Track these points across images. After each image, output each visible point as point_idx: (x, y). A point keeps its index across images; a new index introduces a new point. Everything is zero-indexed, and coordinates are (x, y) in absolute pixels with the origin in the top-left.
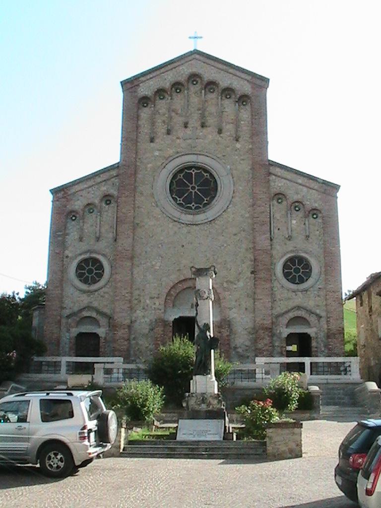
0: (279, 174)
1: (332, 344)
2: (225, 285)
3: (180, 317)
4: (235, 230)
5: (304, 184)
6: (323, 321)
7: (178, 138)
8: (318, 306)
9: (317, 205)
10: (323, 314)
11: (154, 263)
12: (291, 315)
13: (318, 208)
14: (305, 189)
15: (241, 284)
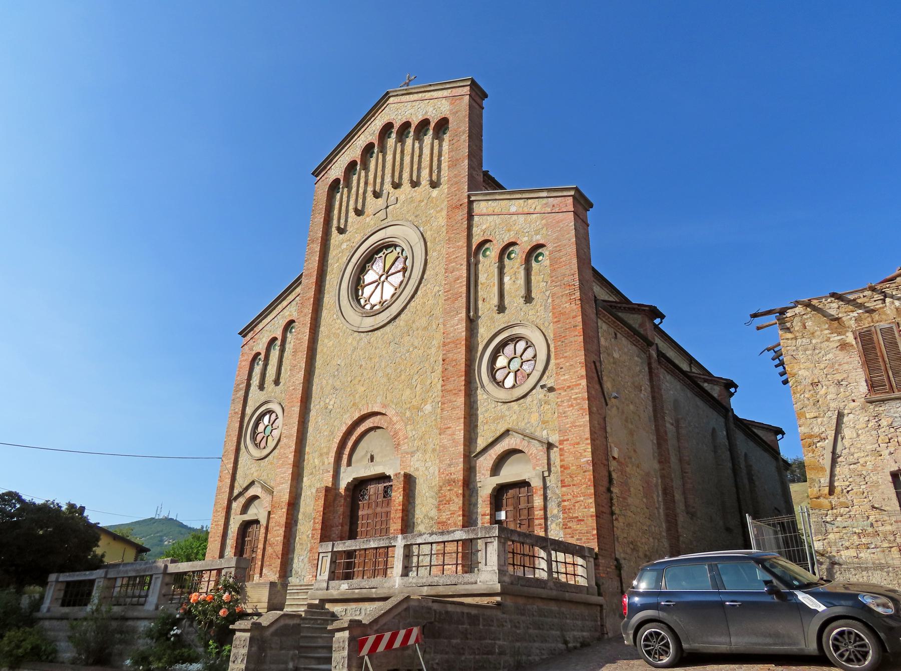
0: (485, 211)
1: (570, 497)
2: (408, 414)
3: (354, 479)
4: (424, 322)
5: (521, 211)
6: (555, 454)
7: (368, 216)
8: (544, 422)
9: (538, 237)
10: (554, 438)
11: (327, 401)
12: (499, 449)
13: (541, 242)
14: (521, 218)
15: (428, 408)
